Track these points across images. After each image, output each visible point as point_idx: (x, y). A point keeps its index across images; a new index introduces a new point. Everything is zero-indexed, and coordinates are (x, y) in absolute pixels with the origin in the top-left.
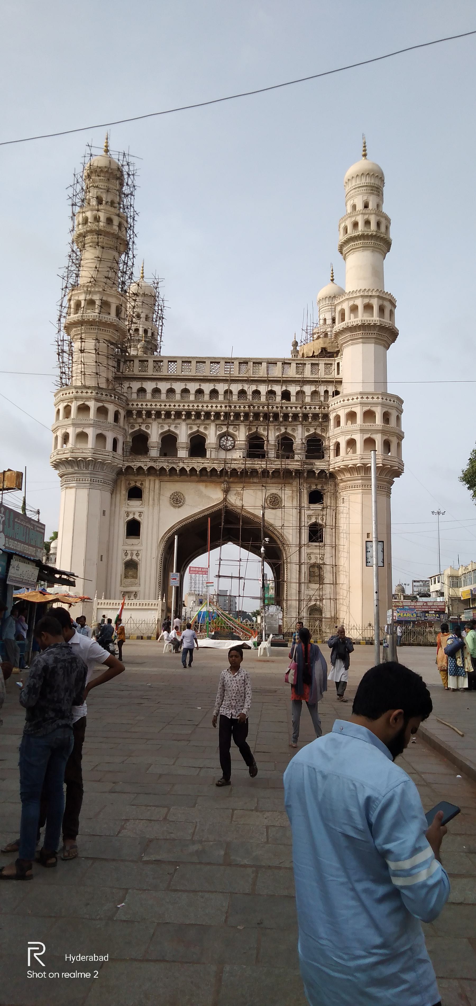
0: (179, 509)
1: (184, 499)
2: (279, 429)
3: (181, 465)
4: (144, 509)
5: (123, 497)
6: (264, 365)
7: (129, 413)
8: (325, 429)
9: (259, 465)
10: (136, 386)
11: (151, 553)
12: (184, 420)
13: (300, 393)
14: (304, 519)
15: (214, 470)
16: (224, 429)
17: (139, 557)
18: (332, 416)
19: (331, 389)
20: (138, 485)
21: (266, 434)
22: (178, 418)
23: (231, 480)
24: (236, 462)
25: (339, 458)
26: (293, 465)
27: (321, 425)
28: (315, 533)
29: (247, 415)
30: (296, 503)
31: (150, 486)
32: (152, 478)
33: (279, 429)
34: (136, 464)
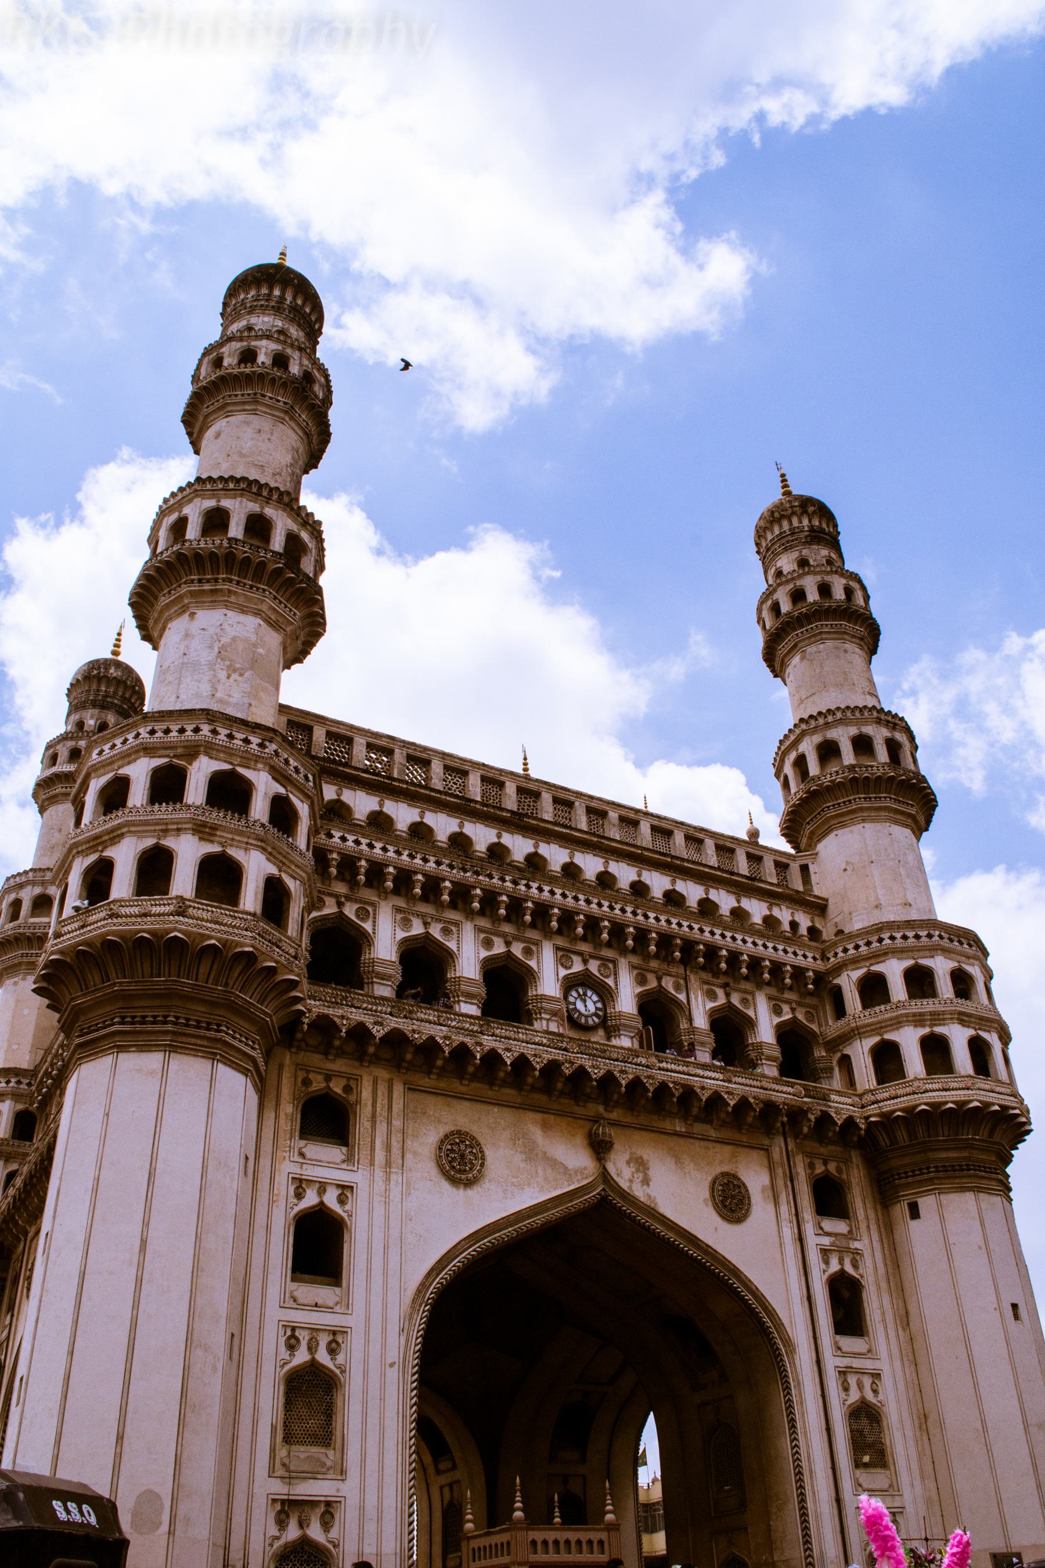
0: (470, 1192)
1: (483, 1158)
4: (357, 1177)
5: (285, 1126)
11: (384, 1345)
12: (470, 914)
14: (814, 1257)
15: (581, 1073)
17: (340, 1359)
19: (804, 921)
20: (337, 1087)
21: (685, 1001)
23: (614, 1115)
24: (639, 1060)
32: (383, 1074)
33: (711, 995)
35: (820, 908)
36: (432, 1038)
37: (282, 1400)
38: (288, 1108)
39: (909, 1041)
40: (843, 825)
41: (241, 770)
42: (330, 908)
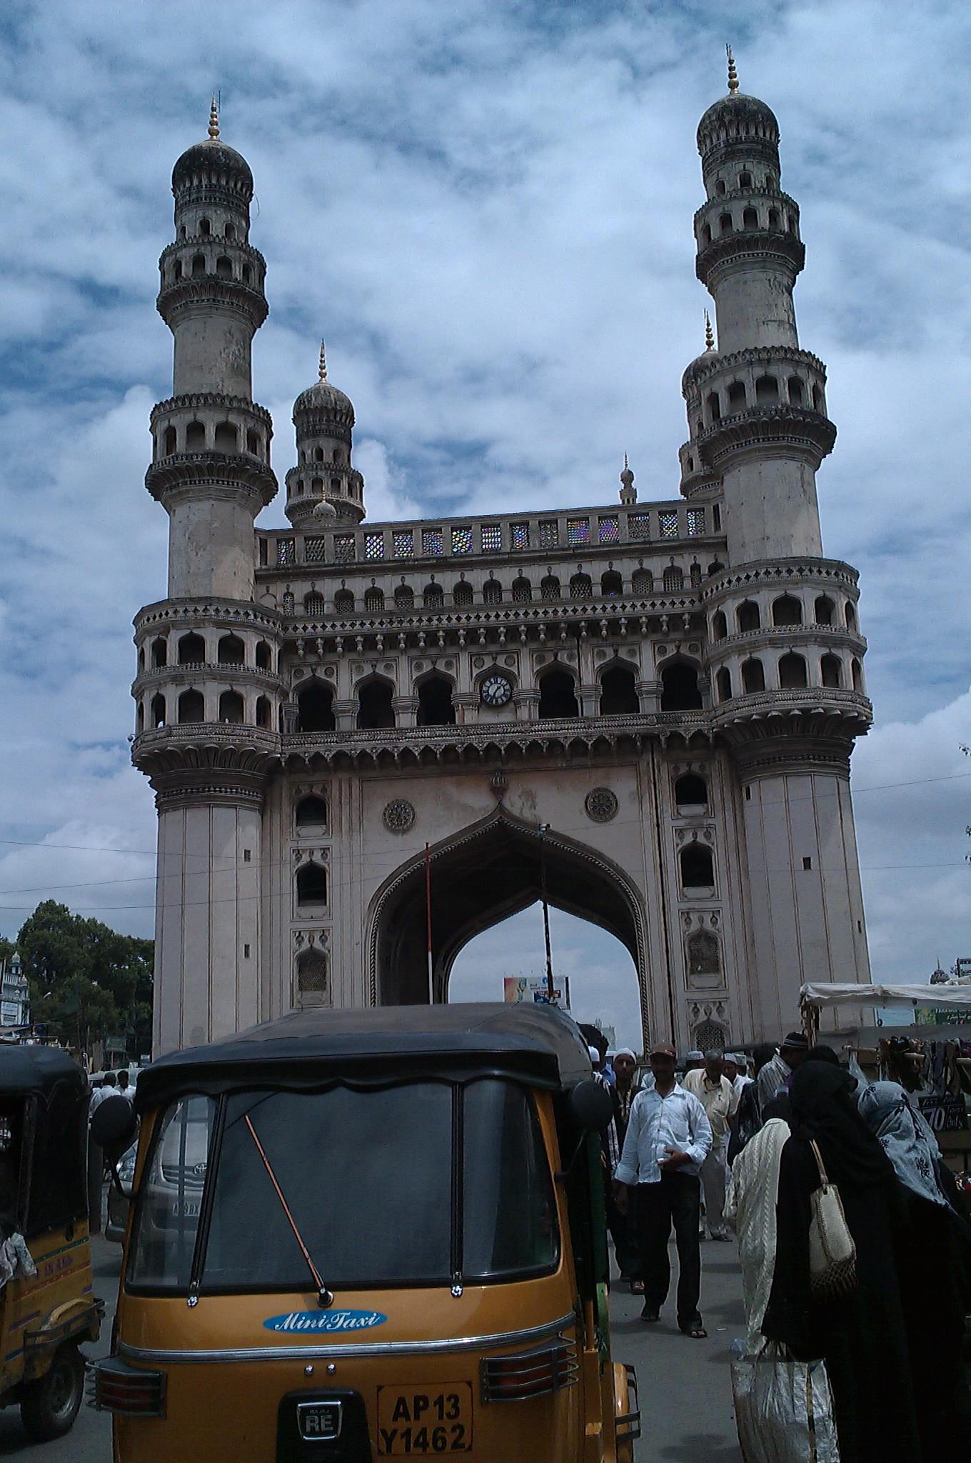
2: (602, 654)
3: (403, 744)
4: (332, 842)
5: (286, 821)
7: (288, 648)
9: (566, 730)
10: (301, 589)
12: (403, 651)
15: (470, 749)
16: (488, 663)
18: (711, 615)
19: (705, 561)
20: (317, 791)
22: (391, 648)
23: (510, 766)
25: (733, 705)
28: (697, 866)
32: (344, 776)
33: (602, 654)
35: (722, 545)
36: (363, 751)
37: (296, 971)
38: (286, 809)
39: (735, 667)
40: (728, 470)
41: (195, 631)
42: (307, 674)
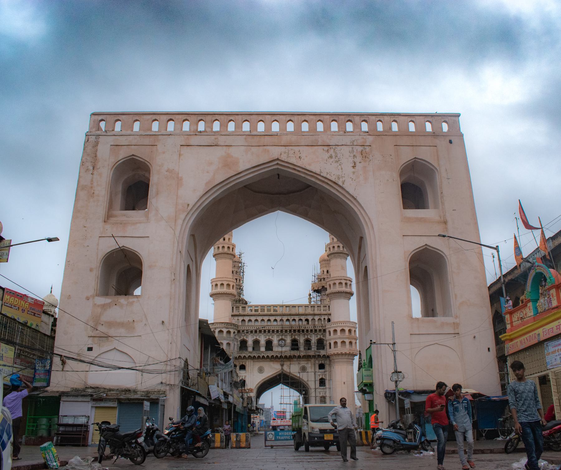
6: (297, 308)
7: (239, 331)
8: (324, 336)
10: (241, 318)
13: (313, 319)
16: (280, 337)
18: (327, 331)
20: (244, 363)
26: (311, 353)
27: (322, 334)
28: (322, 382)
29: (290, 331)
30: (313, 370)
31: (249, 364)
32: (250, 360)
34: (242, 355)
35: (330, 314)
42: (242, 338)
